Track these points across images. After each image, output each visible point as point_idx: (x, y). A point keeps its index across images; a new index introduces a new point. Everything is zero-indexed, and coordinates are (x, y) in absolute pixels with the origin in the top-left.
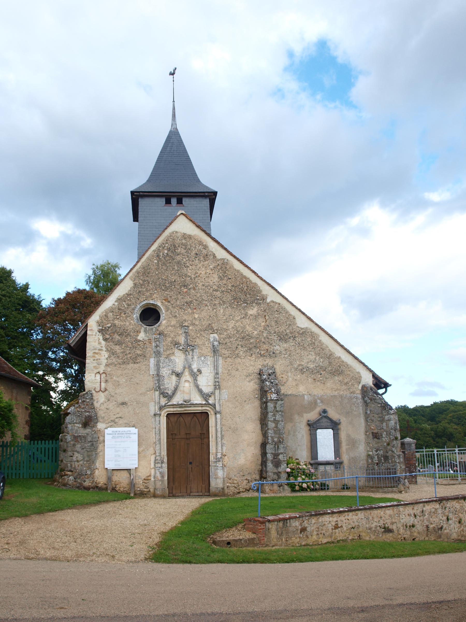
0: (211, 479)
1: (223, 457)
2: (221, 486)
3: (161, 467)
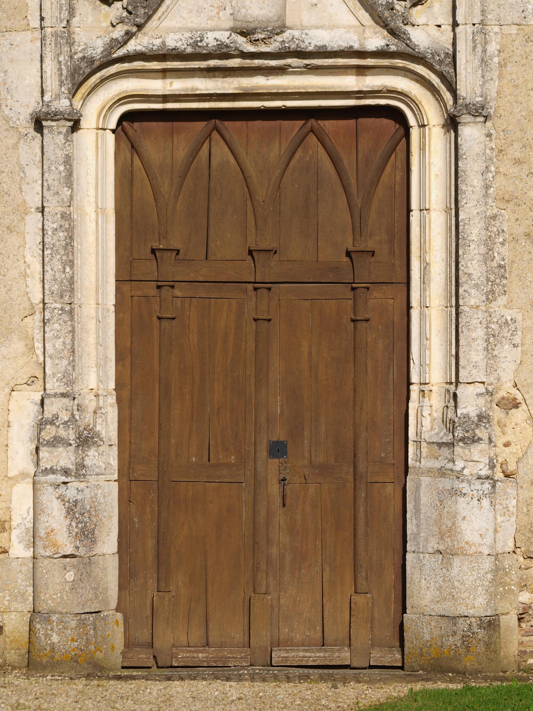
0: (409, 556)
1: (497, 414)
2: (477, 605)
3: (80, 470)
